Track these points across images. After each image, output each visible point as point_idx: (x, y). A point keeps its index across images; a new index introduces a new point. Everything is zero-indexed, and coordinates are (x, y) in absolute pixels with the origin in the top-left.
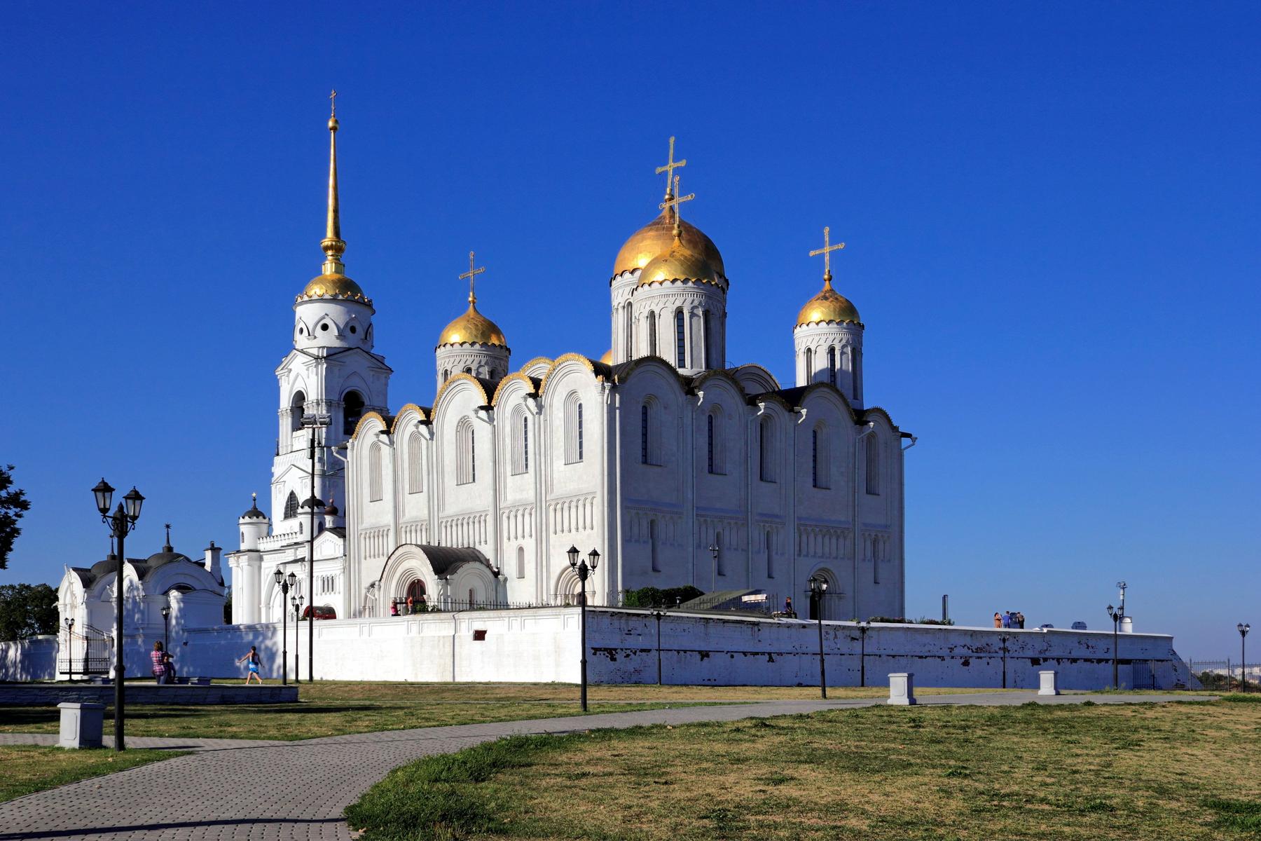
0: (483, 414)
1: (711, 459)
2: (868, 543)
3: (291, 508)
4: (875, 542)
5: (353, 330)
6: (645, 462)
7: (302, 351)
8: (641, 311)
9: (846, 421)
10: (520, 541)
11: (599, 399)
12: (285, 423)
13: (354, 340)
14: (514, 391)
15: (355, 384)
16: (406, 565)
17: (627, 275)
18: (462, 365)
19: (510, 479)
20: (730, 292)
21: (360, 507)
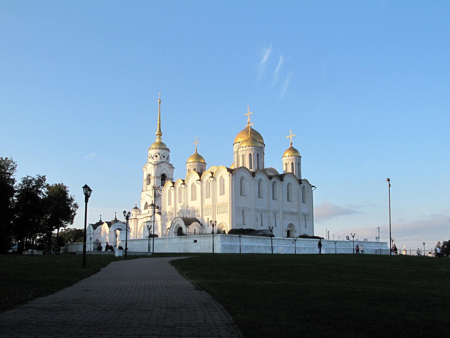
0: (199, 182)
1: (259, 194)
2: (303, 217)
3: (146, 207)
4: (305, 216)
5: (164, 157)
6: (241, 195)
7: (150, 163)
8: (240, 154)
9: (297, 183)
10: (208, 216)
11: (229, 178)
12: (145, 183)
13: (164, 160)
14: (207, 176)
15: (164, 172)
16: (177, 223)
17: (238, 143)
18: (193, 168)
19: (205, 199)
20: (265, 148)
21: (165, 206)
